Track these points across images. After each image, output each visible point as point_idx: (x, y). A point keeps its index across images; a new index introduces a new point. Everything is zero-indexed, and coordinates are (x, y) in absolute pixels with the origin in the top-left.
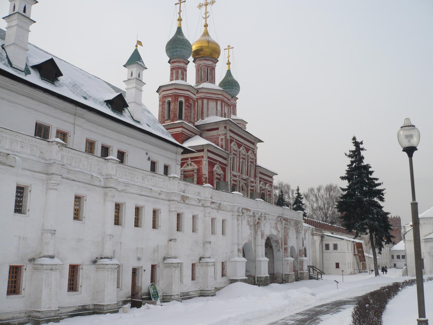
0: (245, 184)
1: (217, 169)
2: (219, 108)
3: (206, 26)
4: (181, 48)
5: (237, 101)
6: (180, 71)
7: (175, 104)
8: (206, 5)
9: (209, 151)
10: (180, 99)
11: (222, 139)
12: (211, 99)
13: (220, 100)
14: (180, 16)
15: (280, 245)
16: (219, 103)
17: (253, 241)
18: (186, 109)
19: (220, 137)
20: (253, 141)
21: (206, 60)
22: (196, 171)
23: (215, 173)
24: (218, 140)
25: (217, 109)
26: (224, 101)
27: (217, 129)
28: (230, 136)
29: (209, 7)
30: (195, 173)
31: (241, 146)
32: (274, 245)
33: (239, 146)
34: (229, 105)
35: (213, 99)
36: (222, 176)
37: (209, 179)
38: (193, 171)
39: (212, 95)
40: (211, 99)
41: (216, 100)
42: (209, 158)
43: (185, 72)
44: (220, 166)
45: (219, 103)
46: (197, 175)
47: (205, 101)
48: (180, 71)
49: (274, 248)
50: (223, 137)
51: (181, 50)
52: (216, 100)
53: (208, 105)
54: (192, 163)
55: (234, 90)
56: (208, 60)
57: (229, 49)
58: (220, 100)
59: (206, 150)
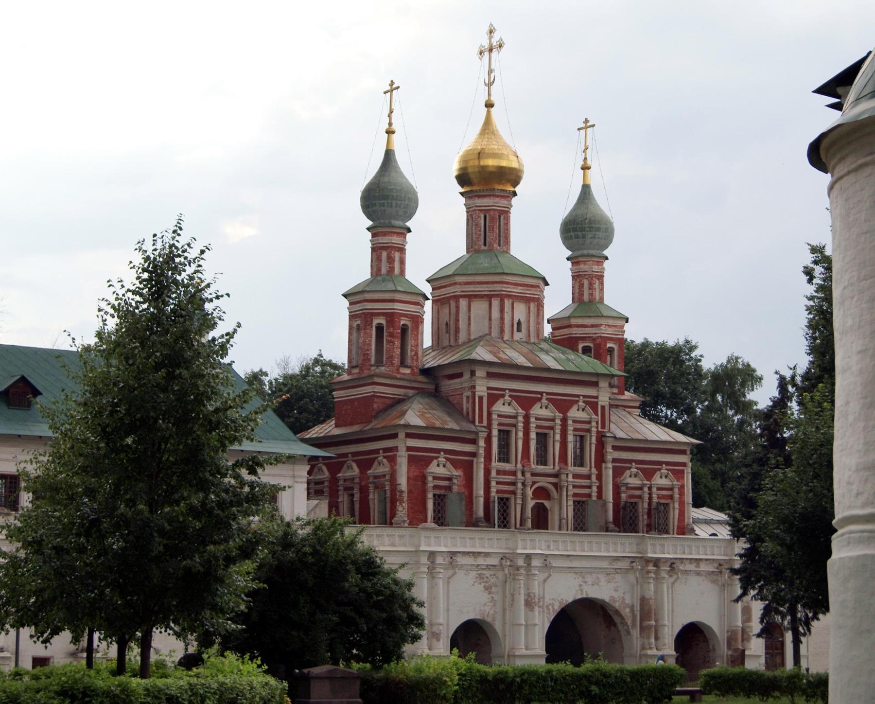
0: (556, 485)
1: (438, 469)
2: (496, 314)
3: (489, 105)
4: (383, 205)
5: (606, 264)
6: (384, 254)
7: (365, 333)
8: (491, 50)
9: (409, 436)
10: (376, 321)
11: (468, 397)
12: (476, 296)
13: (497, 296)
14: (390, 124)
15: (629, 622)
16: (496, 303)
17: (499, 618)
18: (388, 342)
19: (465, 394)
20: (594, 379)
21: (479, 197)
22: (387, 477)
23: (430, 479)
24: (462, 398)
25: (490, 319)
26: (509, 297)
27: (460, 375)
28: (489, 388)
29: (494, 53)
30: (387, 481)
31: (540, 399)
32: (617, 620)
33: (526, 402)
34: (527, 300)
35: (481, 297)
36: (455, 481)
37: (410, 492)
38: (384, 476)
39: (479, 288)
40: (476, 296)
41: (489, 297)
42: (409, 449)
43: (397, 255)
44: (447, 459)
45: (496, 303)
46: (391, 485)
47: (463, 303)
48: (384, 254)
49: (620, 627)
50: (469, 393)
51: (383, 208)
52: (489, 297)
53: (469, 310)
54: (385, 461)
55: (588, 241)
56: (484, 196)
57: (586, 128)
58: (497, 296)
59: (402, 435)
